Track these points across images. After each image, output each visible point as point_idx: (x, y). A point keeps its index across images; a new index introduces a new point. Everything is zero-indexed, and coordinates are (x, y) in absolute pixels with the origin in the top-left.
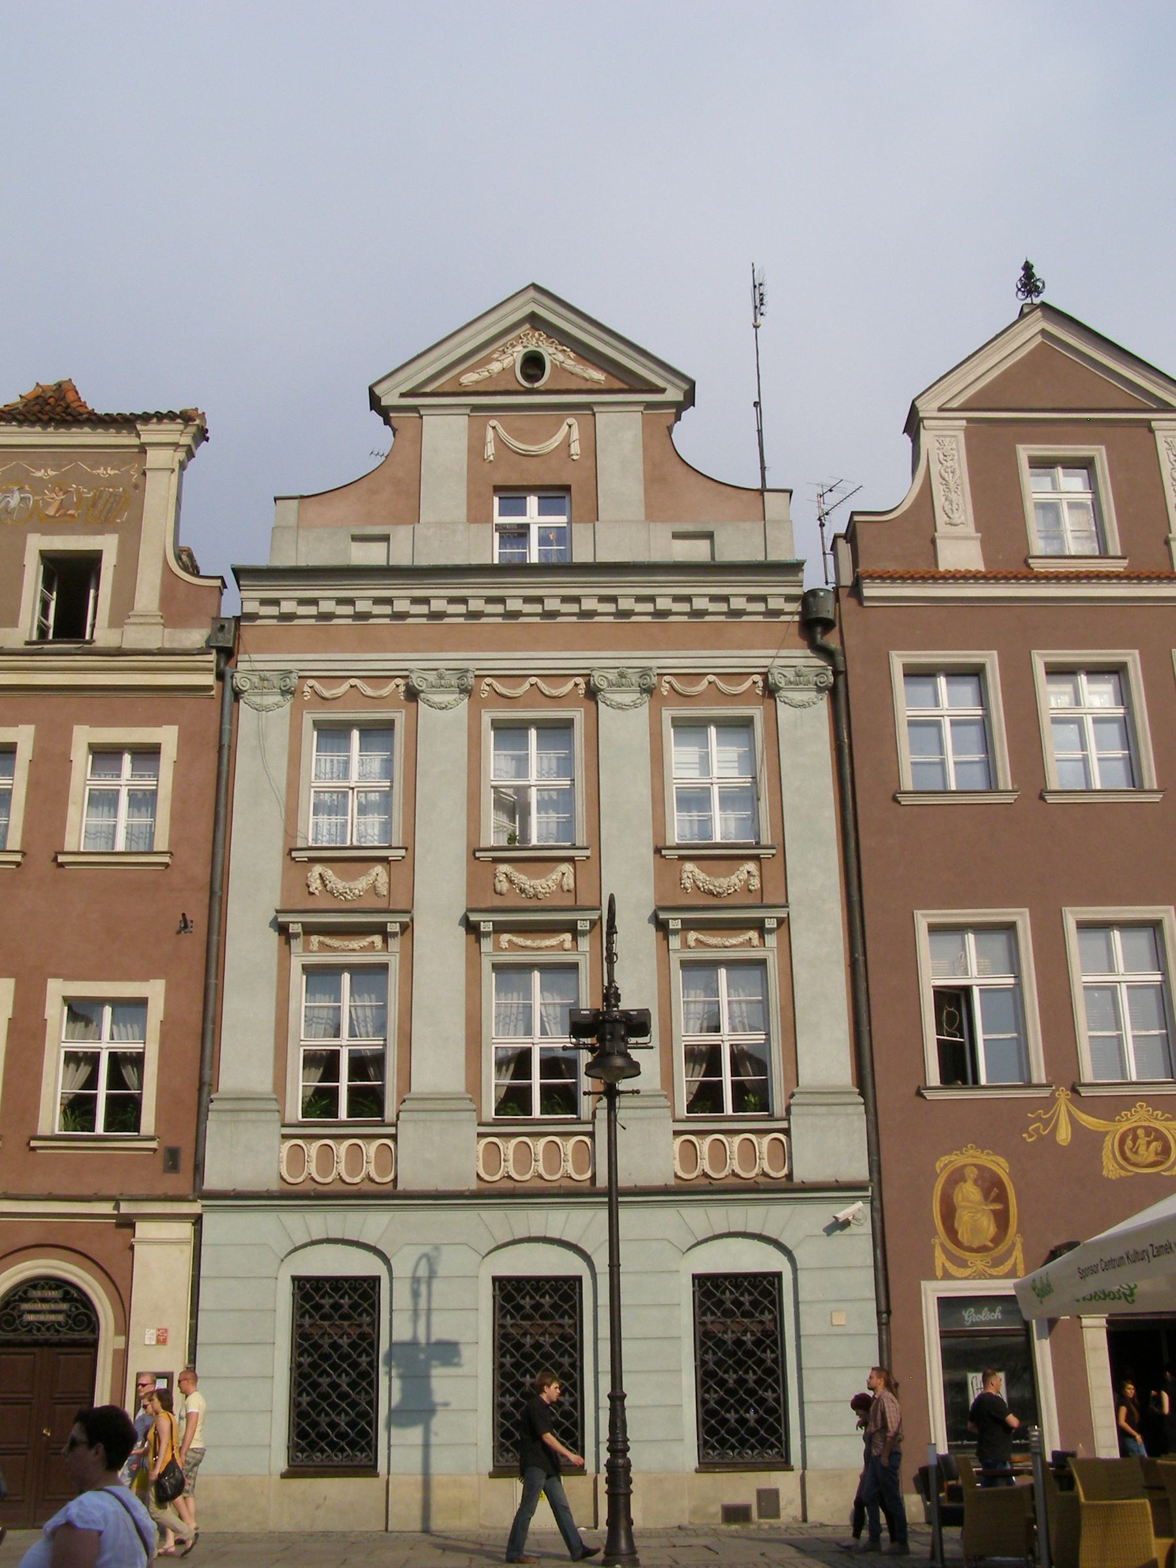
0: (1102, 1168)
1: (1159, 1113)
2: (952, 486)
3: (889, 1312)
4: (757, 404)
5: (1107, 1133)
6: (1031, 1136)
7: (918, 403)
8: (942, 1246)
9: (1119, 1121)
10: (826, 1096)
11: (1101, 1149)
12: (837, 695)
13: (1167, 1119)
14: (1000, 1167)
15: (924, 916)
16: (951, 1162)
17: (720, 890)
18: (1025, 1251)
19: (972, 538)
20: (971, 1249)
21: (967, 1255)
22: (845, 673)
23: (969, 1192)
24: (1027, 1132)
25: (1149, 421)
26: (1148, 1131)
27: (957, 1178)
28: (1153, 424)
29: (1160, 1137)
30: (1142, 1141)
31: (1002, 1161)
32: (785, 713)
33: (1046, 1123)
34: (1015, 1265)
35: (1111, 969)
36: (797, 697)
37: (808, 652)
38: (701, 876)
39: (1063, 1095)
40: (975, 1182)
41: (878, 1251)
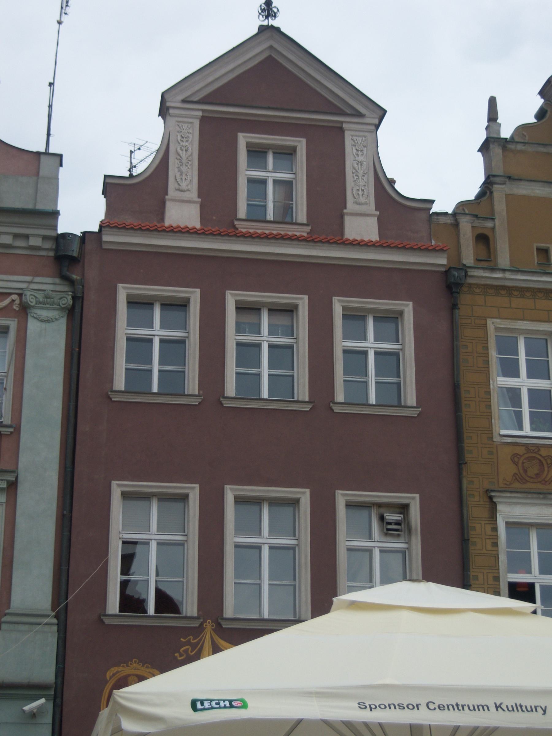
2: (184, 161)
4: (51, 84)
6: (180, 656)
7: (166, 97)
10: (30, 618)
12: (75, 314)
16: (118, 672)
19: (194, 202)
22: (82, 298)
24: (179, 652)
25: (342, 122)
28: (345, 126)
32: (33, 326)
33: (194, 646)
35: (259, 533)
36: (44, 314)
37: (57, 280)
39: (209, 626)
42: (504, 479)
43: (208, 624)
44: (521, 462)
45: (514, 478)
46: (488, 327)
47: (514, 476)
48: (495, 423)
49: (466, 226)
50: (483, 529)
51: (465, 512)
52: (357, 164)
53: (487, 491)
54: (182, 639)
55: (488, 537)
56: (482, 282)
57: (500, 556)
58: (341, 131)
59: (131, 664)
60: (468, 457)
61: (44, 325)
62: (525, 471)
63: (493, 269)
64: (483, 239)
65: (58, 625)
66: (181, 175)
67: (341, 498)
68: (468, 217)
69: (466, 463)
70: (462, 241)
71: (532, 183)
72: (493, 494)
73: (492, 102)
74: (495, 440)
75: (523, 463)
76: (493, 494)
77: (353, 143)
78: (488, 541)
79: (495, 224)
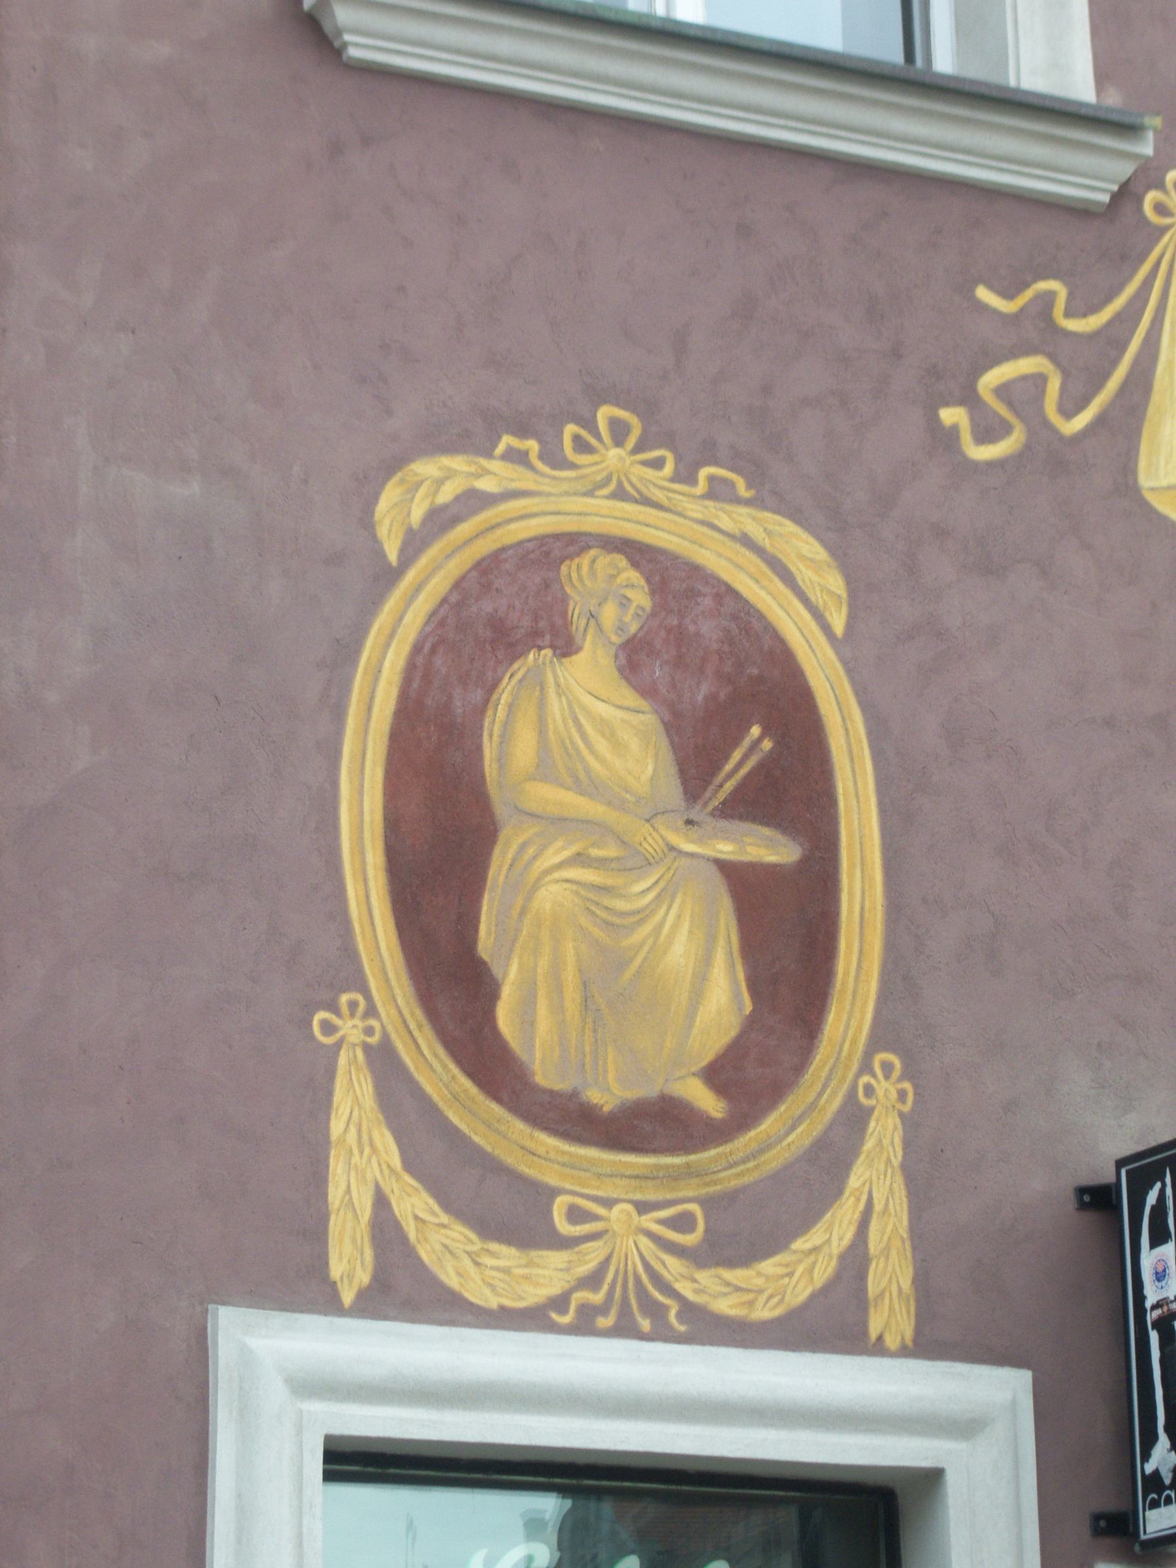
6: (987, 433)
8: (383, 1061)
14: (796, 588)
16: (473, 501)
18: (924, 1174)
20: (576, 1120)
21: (544, 1155)
24: (969, 398)
27: (506, 615)
31: (803, 549)
33: (1087, 364)
34: (855, 1261)
40: (633, 658)
54: (983, 294)
59: (581, 446)
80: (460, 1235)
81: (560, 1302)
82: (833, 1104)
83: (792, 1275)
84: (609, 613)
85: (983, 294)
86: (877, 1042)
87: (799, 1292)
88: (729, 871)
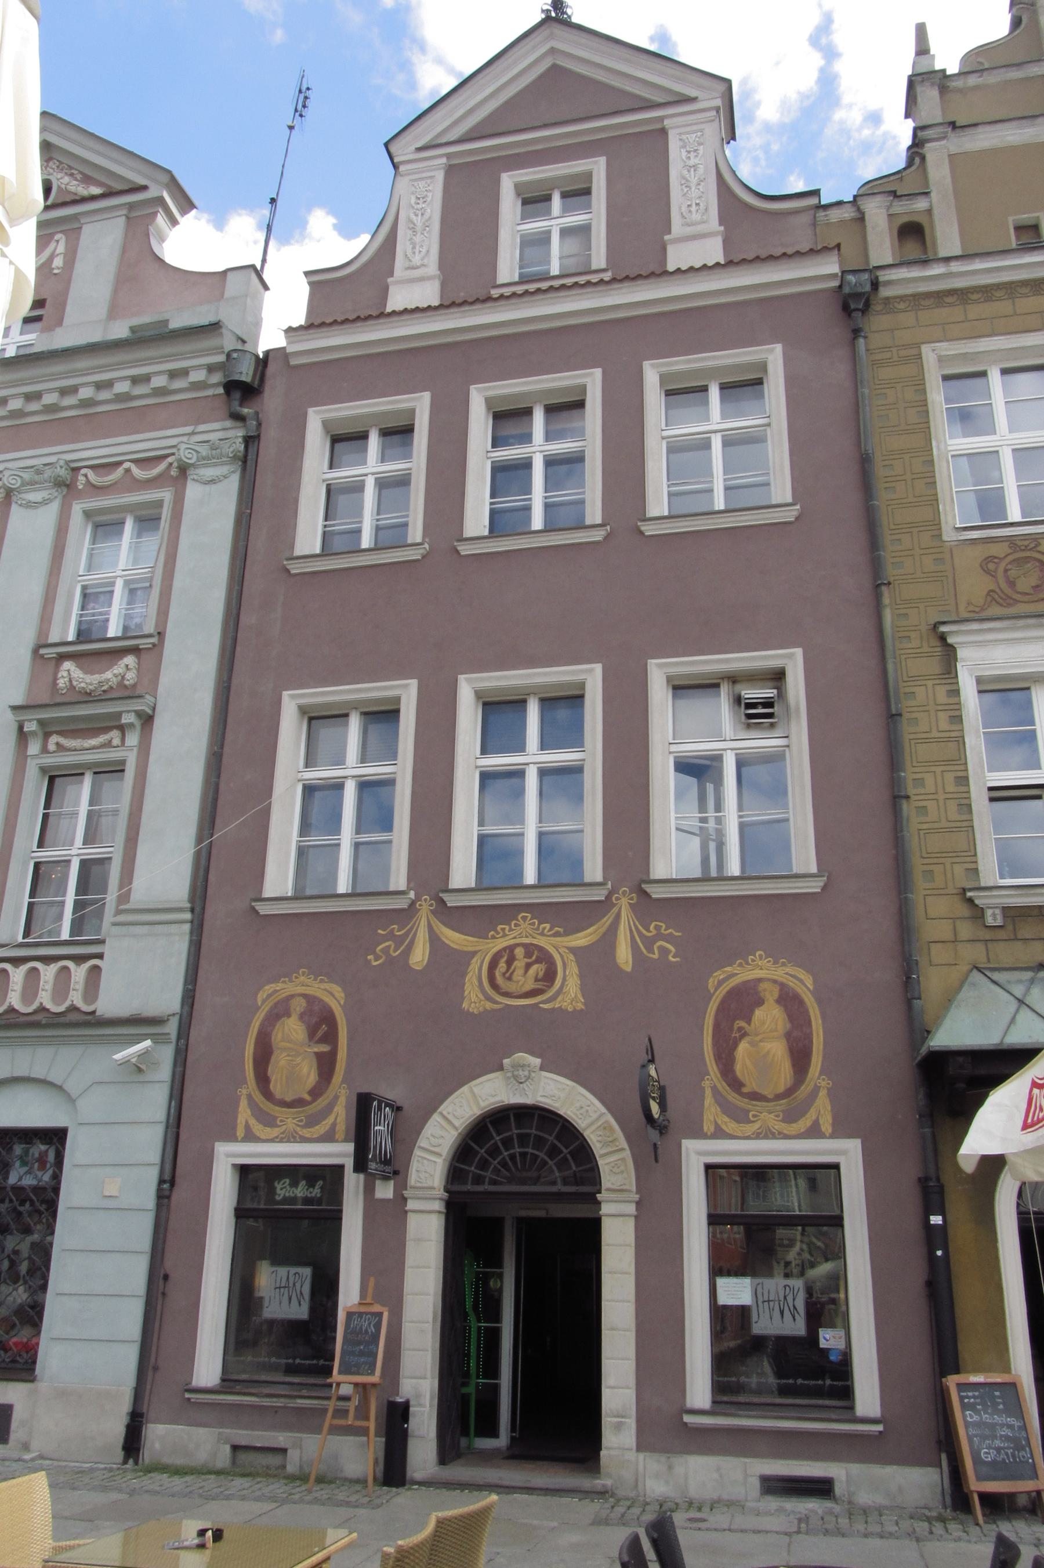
0: (463, 998)
1: (548, 926)
3: (172, 1183)
4: (273, 201)
5: (474, 953)
6: (376, 960)
8: (250, 1097)
9: (493, 937)
10: (155, 915)
11: (464, 974)
13: (557, 934)
14: (333, 996)
15: (292, 697)
16: (276, 991)
17: (91, 687)
23: (292, 1030)
24: (374, 953)
25: (661, 119)
26: (529, 949)
27: (279, 1012)
28: (666, 122)
29: (545, 957)
30: (519, 964)
31: (337, 989)
32: (193, 491)
33: (399, 941)
36: (209, 473)
37: (228, 423)
38: (77, 673)
39: (425, 907)
40: (301, 1017)
41: (173, 1103)
42: (969, 603)
43: (423, 903)
44: (1001, 569)
45: (989, 599)
46: (924, 358)
47: (988, 594)
48: (945, 510)
49: (876, 211)
50: (931, 695)
51: (890, 667)
52: (689, 171)
53: (935, 626)
54: (380, 931)
55: (940, 708)
56: (910, 290)
57: (967, 740)
58: (663, 132)
59: (296, 978)
60: (891, 572)
61: (207, 488)
62: (1012, 584)
63: (925, 262)
64: (912, 233)
65: (192, 922)
66: (414, 248)
67: (658, 675)
68: (879, 198)
69: (889, 583)
70: (871, 237)
71: (999, 126)
72: (943, 629)
73: (921, 31)
74: (945, 538)
75: (1006, 571)
76: (943, 629)
77: (681, 144)
78: (941, 714)
79: (931, 202)
80: (260, 1127)
81: (277, 1137)
82: (331, 1097)
83: (321, 1129)
84: (298, 1009)
85: (380, 931)
86: (343, 1082)
87: (322, 1131)
88: (317, 1054)
